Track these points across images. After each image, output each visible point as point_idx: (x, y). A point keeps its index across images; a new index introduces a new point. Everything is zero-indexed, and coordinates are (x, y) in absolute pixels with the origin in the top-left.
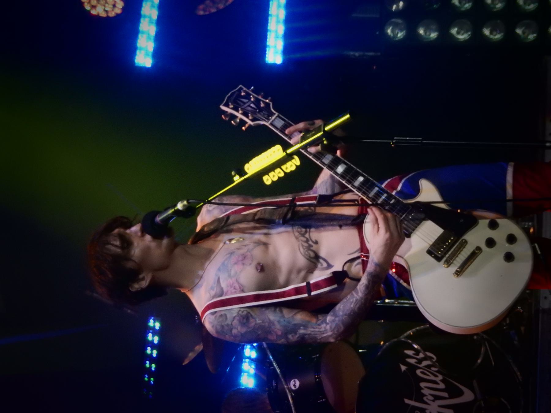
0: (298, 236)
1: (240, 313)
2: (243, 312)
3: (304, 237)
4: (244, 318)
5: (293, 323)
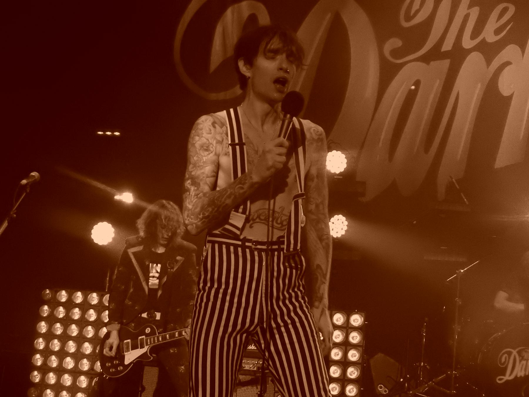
0: (258, 213)
1: (211, 146)
2: (212, 147)
3: (257, 218)
4: (207, 147)
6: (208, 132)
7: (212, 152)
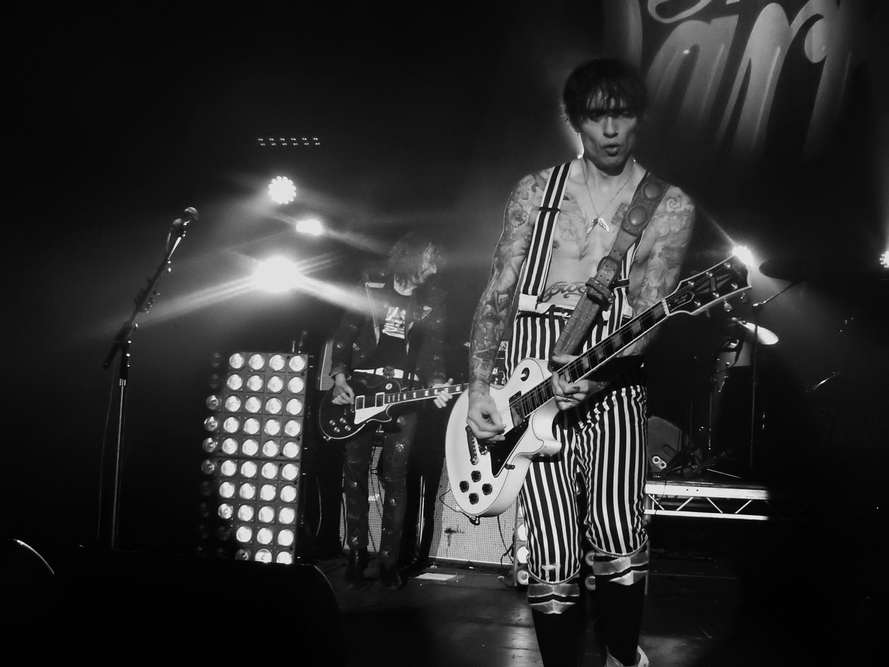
1: (525, 214)
2: (525, 216)
4: (519, 216)
5: (505, 265)
6: (524, 197)
7: (524, 223)
